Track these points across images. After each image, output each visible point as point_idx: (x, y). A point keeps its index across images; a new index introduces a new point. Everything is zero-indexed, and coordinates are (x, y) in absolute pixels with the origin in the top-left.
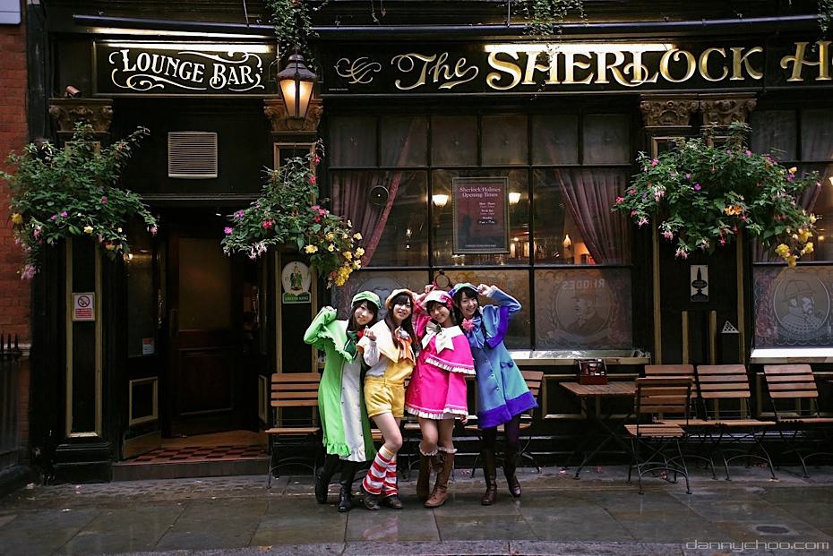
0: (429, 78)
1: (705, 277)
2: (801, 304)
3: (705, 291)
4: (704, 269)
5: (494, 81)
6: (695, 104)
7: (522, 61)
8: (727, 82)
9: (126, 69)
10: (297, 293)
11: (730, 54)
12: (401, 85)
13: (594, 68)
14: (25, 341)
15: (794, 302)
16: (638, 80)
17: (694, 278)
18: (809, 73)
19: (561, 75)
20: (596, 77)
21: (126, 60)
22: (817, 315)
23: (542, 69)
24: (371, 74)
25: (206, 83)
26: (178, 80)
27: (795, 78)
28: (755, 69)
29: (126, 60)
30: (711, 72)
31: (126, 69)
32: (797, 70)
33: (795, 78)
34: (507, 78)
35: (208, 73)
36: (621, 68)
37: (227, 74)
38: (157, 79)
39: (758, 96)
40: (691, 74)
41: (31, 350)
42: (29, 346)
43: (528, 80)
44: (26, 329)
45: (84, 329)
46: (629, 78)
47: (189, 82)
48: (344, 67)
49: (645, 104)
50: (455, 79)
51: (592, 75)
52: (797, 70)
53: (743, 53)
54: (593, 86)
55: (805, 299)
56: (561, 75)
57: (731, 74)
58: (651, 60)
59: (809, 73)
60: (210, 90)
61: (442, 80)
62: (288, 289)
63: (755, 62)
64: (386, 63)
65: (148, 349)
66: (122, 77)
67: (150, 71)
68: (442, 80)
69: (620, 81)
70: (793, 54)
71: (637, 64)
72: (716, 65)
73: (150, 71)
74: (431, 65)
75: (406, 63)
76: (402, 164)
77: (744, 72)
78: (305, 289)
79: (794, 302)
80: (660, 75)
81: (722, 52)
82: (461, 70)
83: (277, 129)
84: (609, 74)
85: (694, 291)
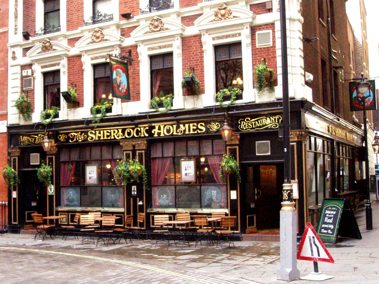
0: (76, 139)
1: (136, 189)
2: (163, 196)
3: (136, 193)
4: (135, 187)
5: (90, 139)
6: (132, 143)
7: (95, 134)
8: (140, 137)
9: (21, 140)
10: (51, 192)
11: (141, 129)
12: (71, 141)
13: (111, 135)
14: (6, 202)
15: (162, 196)
16: (120, 137)
17: (133, 189)
18: (159, 134)
19: (104, 137)
20: (111, 137)
21: (21, 138)
22: (167, 199)
23: (100, 135)
24: (65, 138)
25: (35, 143)
26: (30, 142)
27: (156, 135)
29: (21, 138)
31: (21, 140)
33: (156, 135)
34: (92, 138)
35: (35, 140)
37: (39, 140)
38: (27, 142)
39: (147, 141)
40: (132, 136)
43: (97, 139)
44: (7, 199)
45: (15, 199)
46: (118, 137)
47: (32, 143)
48: (60, 137)
49: (121, 144)
50: (82, 139)
51: (110, 137)
53: (144, 129)
54: (111, 139)
55: (164, 195)
56: (104, 137)
57: (141, 135)
58: (123, 131)
59: (159, 134)
60: (35, 144)
61: (79, 139)
62: (49, 190)
64: (68, 135)
65: (252, 206)
66: (21, 142)
67: (25, 141)
68: (79, 139)
69: (117, 138)
71: (120, 133)
72: (138, 132)
73: (25, 141)
74: (77, 136)
75: (72, 136)
76: (76, 160)
78: (53, 191)
79: (162, 196)
80: (125, 137)
81: (139, 130)
82: (83, 136)
83: (48, 153)
85: (133, 193)
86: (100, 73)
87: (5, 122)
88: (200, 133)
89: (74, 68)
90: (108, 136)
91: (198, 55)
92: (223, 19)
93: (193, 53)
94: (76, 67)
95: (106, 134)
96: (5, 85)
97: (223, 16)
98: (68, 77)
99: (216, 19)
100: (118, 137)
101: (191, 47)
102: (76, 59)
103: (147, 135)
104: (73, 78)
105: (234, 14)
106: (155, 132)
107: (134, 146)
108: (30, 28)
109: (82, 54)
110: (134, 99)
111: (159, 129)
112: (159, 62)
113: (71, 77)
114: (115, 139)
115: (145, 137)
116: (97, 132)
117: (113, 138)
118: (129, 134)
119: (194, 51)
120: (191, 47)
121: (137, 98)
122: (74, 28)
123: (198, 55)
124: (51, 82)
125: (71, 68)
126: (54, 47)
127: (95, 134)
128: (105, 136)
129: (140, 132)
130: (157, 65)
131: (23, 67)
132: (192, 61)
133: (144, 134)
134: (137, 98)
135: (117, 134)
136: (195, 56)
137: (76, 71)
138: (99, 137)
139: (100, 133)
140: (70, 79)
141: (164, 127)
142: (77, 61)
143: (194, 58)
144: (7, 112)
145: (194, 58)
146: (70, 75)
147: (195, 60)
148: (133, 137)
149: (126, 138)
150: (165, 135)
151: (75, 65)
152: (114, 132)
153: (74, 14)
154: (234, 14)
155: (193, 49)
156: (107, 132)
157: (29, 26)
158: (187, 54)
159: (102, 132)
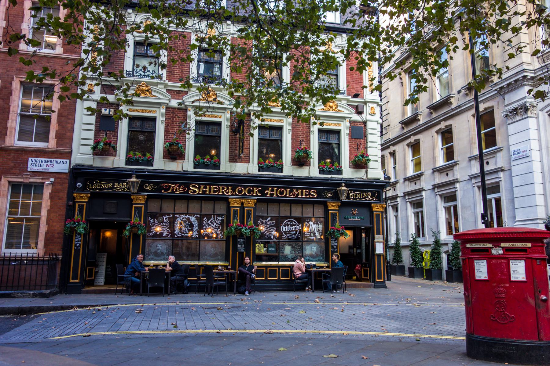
7: (199, 188)
11: (253, 189)
16: (230, 194)
18: (272, 195)
19: (210, 191)
20: (219, 192)
28: (260, 193)
30: (248, 193)
32: (269, 194)
36: (226, 191)
40: (243, 193)
41: (62, 258)
42: (61, 257)
52: (269, 194)
53: (256, 189)
56: (210, 191)
57: (253, 194)
63: (259, 191)
70: (268, 190)
72: (249, 192)
77: (256, 193)
83: (134, 202)
84: (223, 192)
86: (214, 131)
87: (68, 161)
88: (312, 198)
89: (173, 119)
90: (214, 191)
91: (305, 134)
92: (331, 110)
93: (300, 132)
94: (176, 119)
95: (212, 189)
96: (69, 119)
97: (331, 107)
98: (165, 127)
99: (325, 108)
100: (227, 193)
101: (299, 126)
102: (176, 111)
103: (259, 195)
104: (173, 129)
105: (339, 108)
106: (267, 192)
107: (242, 204)
108: (114, 65)
109: (188, 108)
110: (242, 160)
111: (272, 190)
112: (266, 132)
113: (169, 128)
114: (224, 194)
115: (257, 196)
116: (202, 187)
117: (221, 193)
118: (240, 192)
119: (302, 130)
120: (299, 126)
121: (247, 160)
122: (176, 80)
123: (305, 134)
124: (138, 128)
125: (170, 119)
126: (153, 93)
127: (199, 188)
128: (212, 191)
129: (253, 191)
130: (264, 134)
131: (100, 105)
132: (299, 137)
133: (256, 193)
134: (247, 160)
135: (226, 191)
136: (301, 134)
137: (176, 123)
138: (204, 192)
139: (205, 188)
140: (167, 129)
141: (277, 190)
142: (178, 113)
143: (301, 135)
144: (72, 150)
145: (301, 135)
146: (168, 125)
147: (302, 138)
148: (245, 194)
149: (236, 195)
150: (278, 196)
151: (175, 117)
152: (223, 188)
153: (176, 67)
154: (339, 108)
155: (300, 128)
156: (214, 188)
157: (114, 63)
158: (295, 131)
159: (208, 187)
